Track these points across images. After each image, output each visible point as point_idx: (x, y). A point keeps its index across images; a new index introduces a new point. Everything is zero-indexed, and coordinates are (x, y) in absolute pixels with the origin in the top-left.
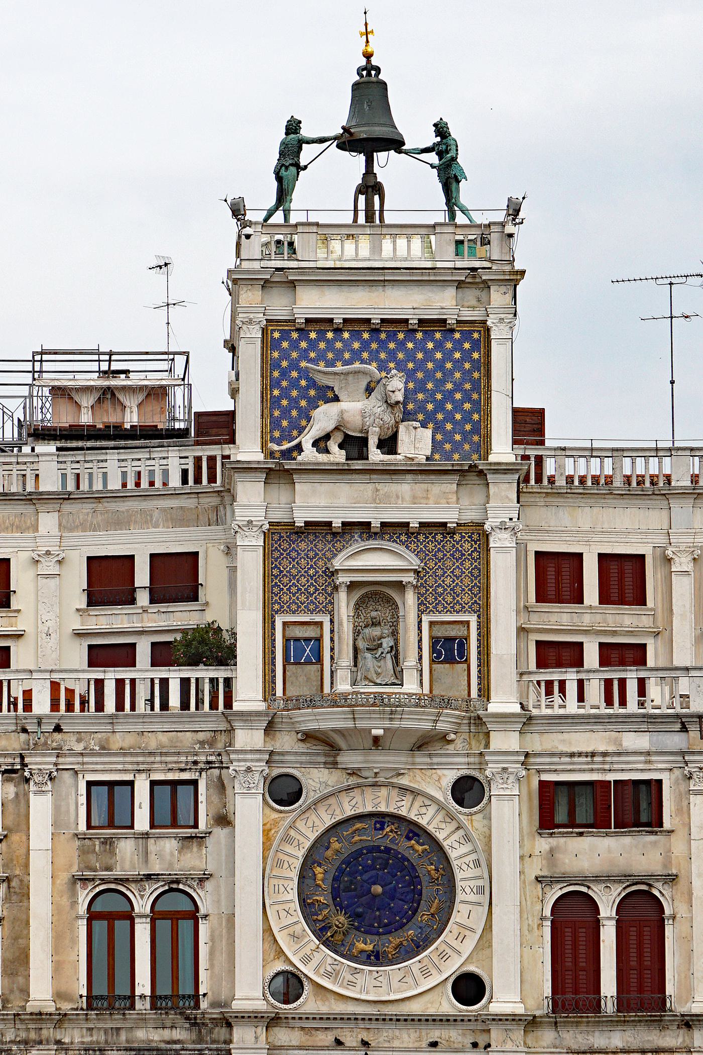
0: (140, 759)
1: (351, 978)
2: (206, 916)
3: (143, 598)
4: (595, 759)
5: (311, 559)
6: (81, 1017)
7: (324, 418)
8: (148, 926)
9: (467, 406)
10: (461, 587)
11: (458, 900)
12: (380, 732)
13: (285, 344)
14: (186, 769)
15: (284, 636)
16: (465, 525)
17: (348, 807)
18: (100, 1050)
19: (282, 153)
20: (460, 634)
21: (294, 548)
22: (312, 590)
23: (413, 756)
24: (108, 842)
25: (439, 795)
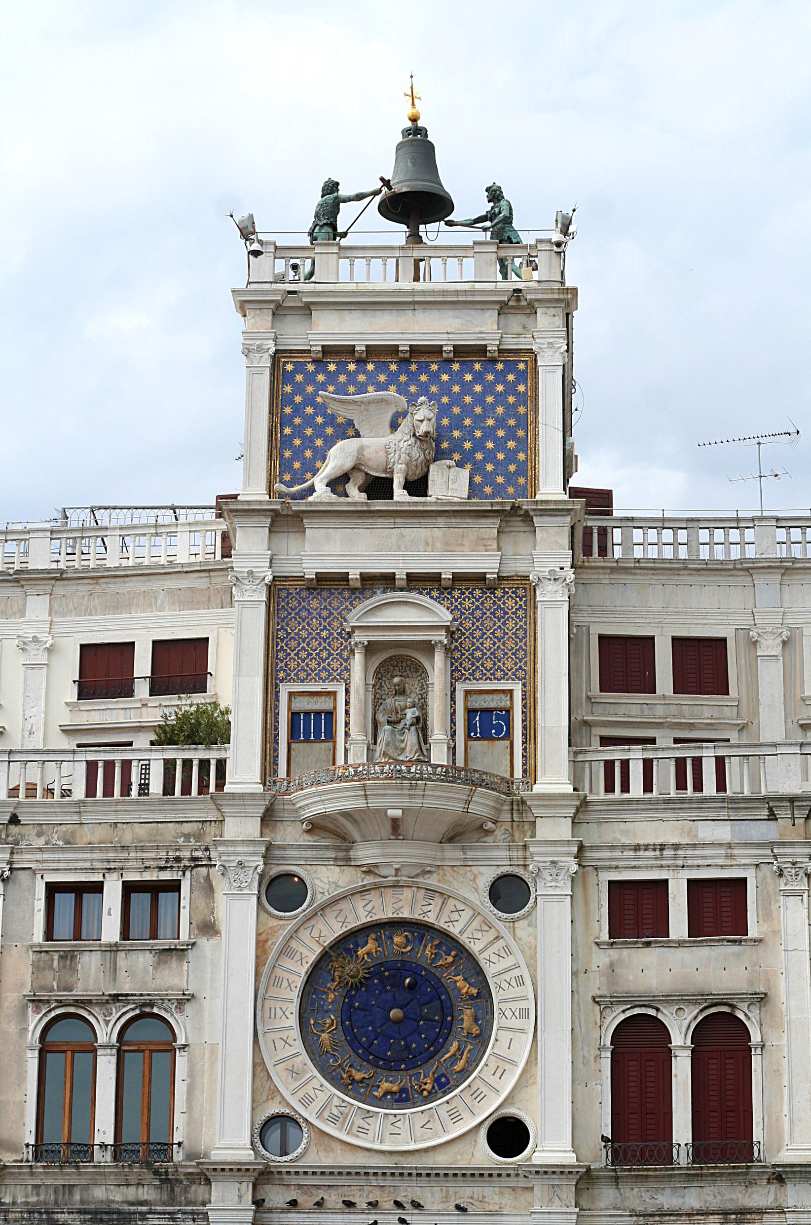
0: (111, 855)
1: (363, 1123)
2: (184, 1047)
3: (142, 689)
4: (665, 853)
5: (325, 620)
6: (24, 1170)
7: (339, 457)
8: (114, 1060)
9: (511, 444)
10: (503, 650)
12: (398, 813)
13: (299, 378)
14: (166, 868)
15: (289, 708)
16: (508, 578)
17: (362, 913)
18: (47, 1212)
19: (317, 216)
20: (502, 705)
21: (304, 607)
22: (324, 654)
23: (443, 851)
24: (68, 957)
25: (473, 897)
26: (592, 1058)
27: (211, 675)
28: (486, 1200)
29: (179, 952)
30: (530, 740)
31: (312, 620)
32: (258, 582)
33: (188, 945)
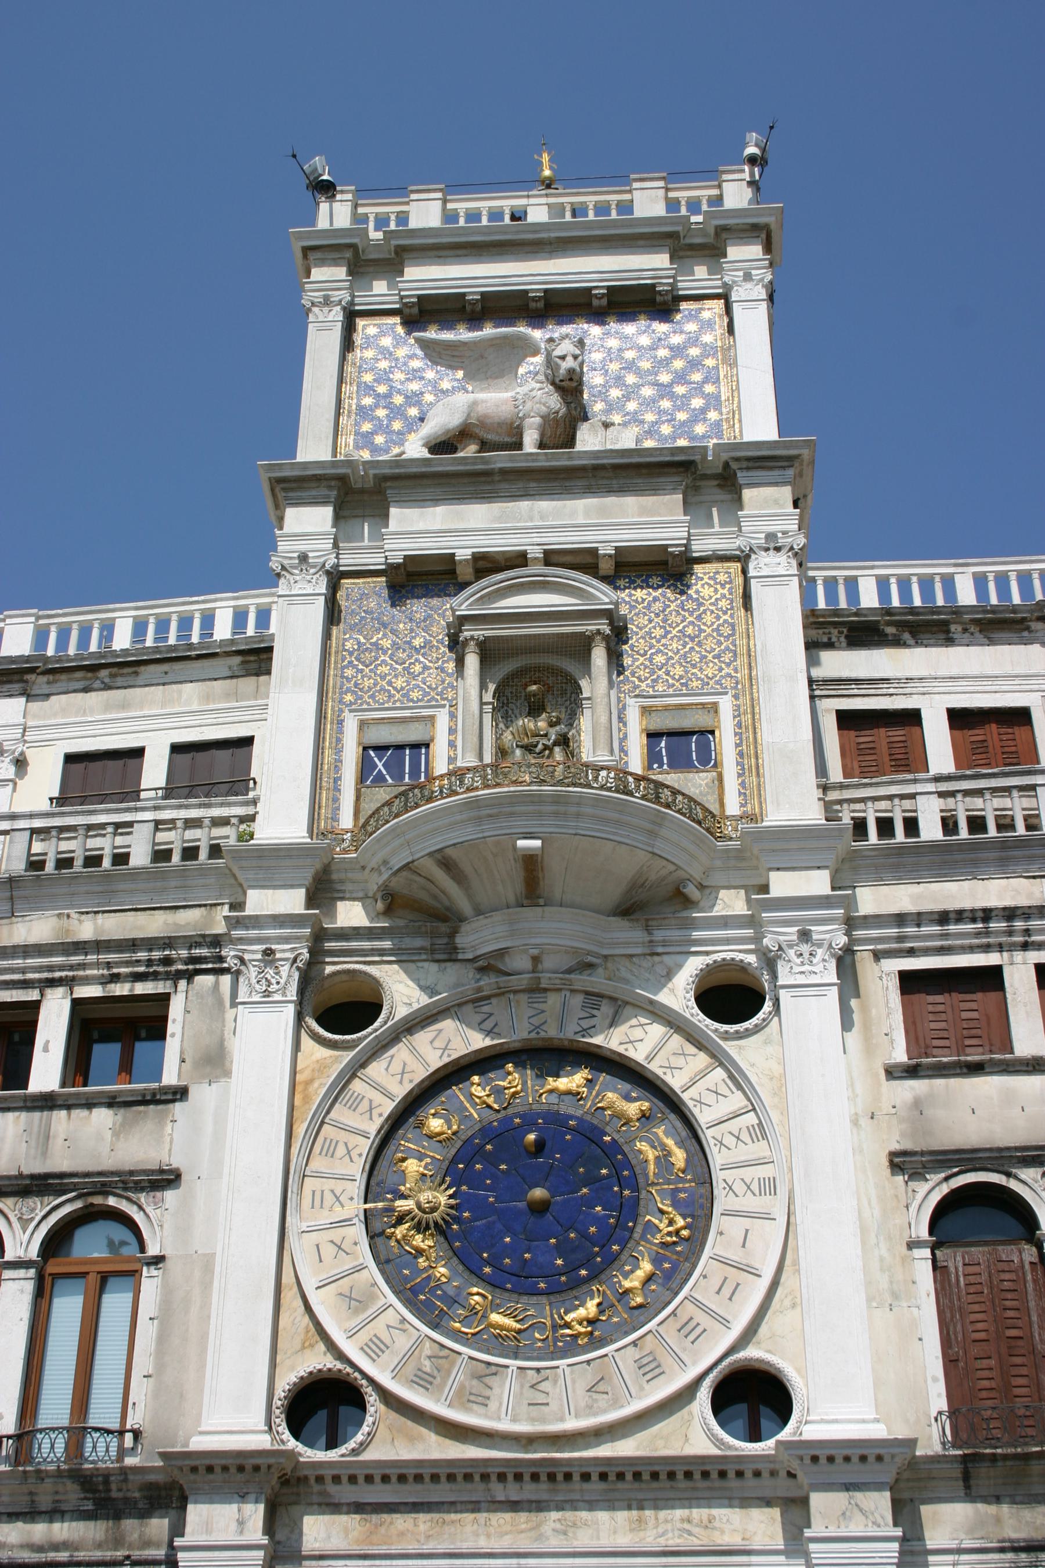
2: (158, 1260)
11: (717, 1209)
15: (359, 744)
22: (418, 668)
27: (255, 783)
28: (717, 1524)
29: (160, 1107)
30: (750, 770)
32: (312, 571)
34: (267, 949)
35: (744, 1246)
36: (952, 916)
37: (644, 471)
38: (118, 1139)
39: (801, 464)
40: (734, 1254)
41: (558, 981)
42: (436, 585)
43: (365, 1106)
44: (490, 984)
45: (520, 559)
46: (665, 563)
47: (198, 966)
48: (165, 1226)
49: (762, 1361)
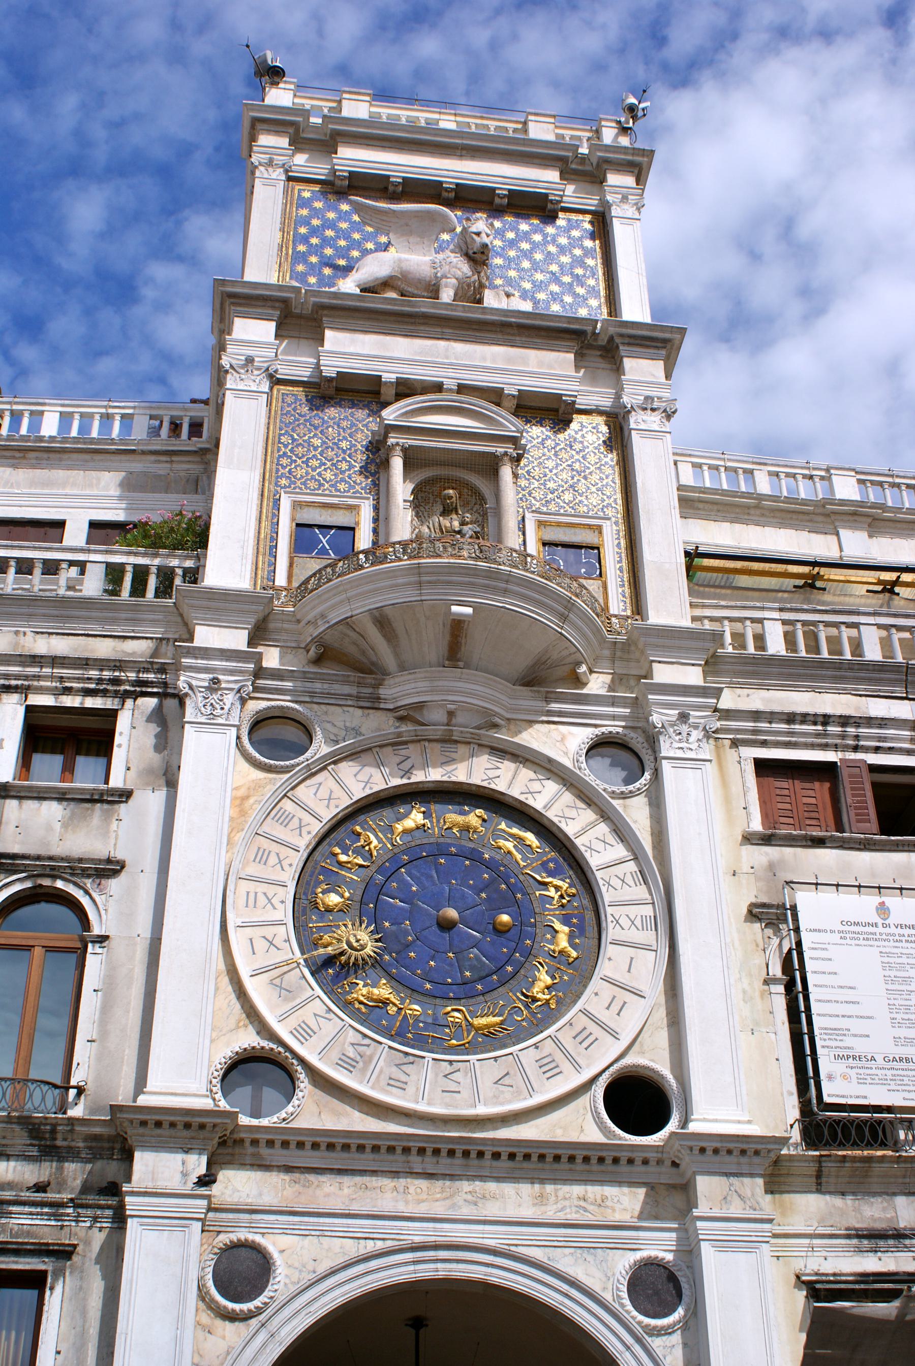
2: (102, 939)
12: (469, 610)
15: (293, 519)
26: (757, 994)
28: (609, 1203)
29: (106, 806)
31: (327, 428)
33: (121, 796)
34: (214, 678)
35: (629, 971)
36: (798, 718)
37: (543, 333)
38: (66, 831)
39: (672, 348)
40: (620, 976)
41: (469, 735)
42: (360, 401)
43: (295, 823)
44: (409, 731)
45: (438, 388)
46: (556, 410)
47: (144, 689)
48: (110, 910)
49: (648, 1068)
